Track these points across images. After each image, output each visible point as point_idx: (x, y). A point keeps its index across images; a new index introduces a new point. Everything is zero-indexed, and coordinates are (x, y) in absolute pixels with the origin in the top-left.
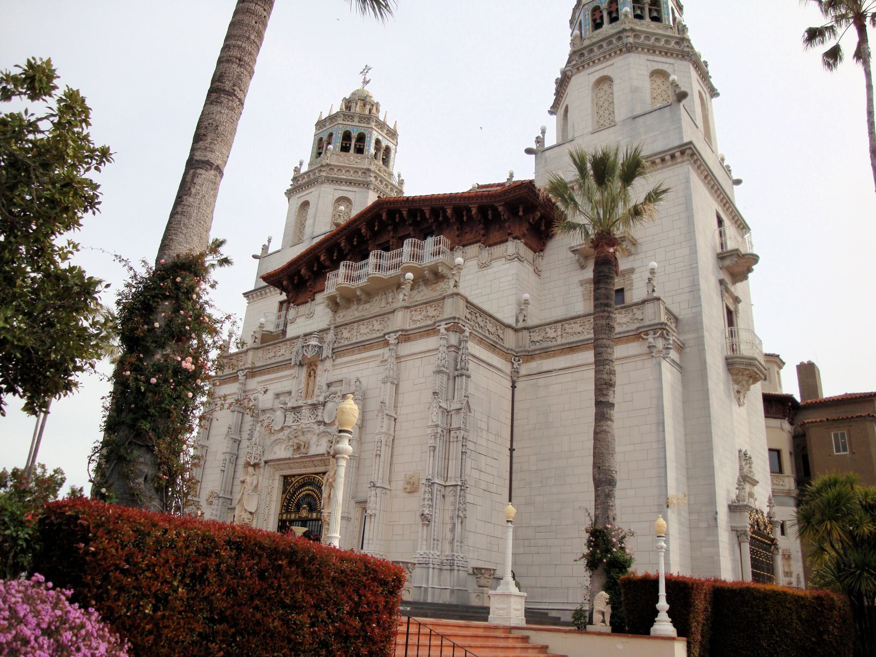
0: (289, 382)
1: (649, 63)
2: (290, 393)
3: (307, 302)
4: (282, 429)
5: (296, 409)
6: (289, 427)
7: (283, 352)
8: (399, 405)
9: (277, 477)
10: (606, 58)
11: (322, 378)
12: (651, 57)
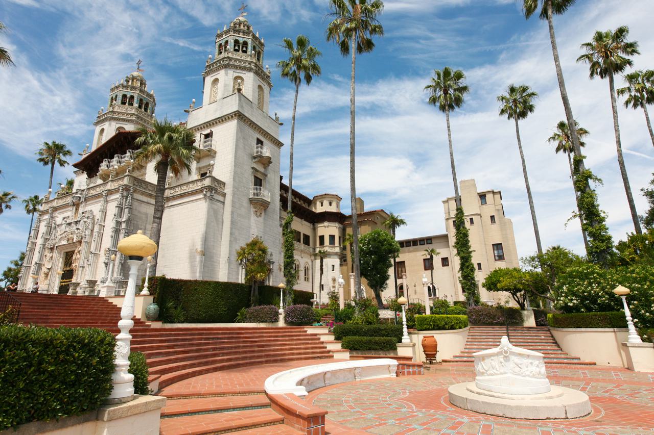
0: (69, 213)
1: (234, 73)
2: (69, 217)
3: (94, 177)
4: (65, 232)
5: (70, 224)
6: (66, 231)
7: (69, 200)
8: (106, 220)
9: (62, 253)
10: (218, 69)
11: (81, 210)
12: (235, 71)
